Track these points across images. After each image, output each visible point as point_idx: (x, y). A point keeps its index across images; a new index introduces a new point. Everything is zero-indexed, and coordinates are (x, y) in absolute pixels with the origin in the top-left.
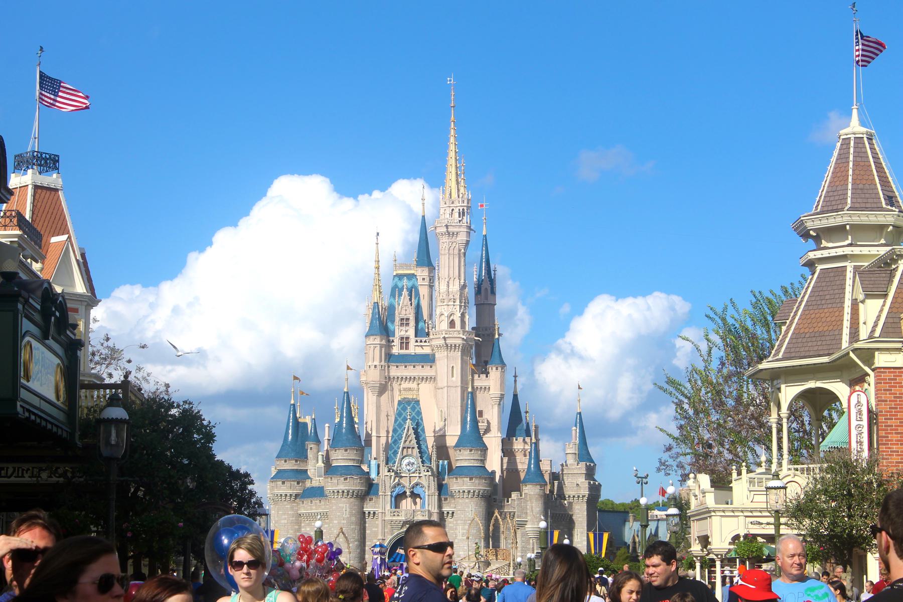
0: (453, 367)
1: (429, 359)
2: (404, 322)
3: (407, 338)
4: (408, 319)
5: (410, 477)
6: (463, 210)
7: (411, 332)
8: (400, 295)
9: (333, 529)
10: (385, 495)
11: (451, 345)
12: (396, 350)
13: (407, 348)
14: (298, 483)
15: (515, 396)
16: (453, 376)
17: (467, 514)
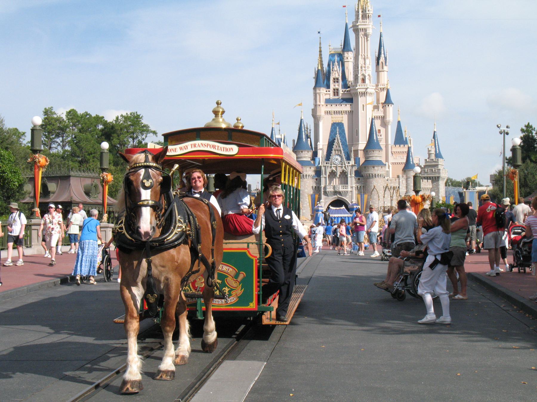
2: (336, 80)
3: (337, 90)
4: (338, 79)
5: (339, 167)
6: (368, 15)
8: (333, 65)
12: (332, 97)
13: (338, 95)
15: (399, 122)
16: (363, 110)
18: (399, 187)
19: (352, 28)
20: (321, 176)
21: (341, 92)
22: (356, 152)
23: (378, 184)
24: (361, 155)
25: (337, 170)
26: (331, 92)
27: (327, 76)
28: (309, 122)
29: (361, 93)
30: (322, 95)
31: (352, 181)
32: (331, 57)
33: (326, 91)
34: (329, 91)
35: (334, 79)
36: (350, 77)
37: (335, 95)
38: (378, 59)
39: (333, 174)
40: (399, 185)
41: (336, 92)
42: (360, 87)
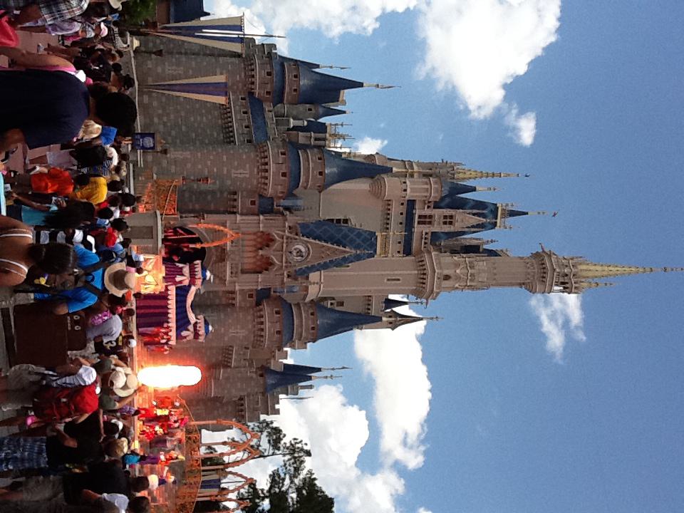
0: (399, 280)
1: (407, 251)
2: (449, 220)
4: (451, 223)
7: (436, 228)
9: (214, 153)
10: (259, 223)
11: (425, 279)
12: (417, 212)
14: (268, 93)
16: (388, 280)
17: (233, 328)
18: (230, 367)
19: (540, 251)
20: (261, 217)
21: (426, 229)
25: (274, 250)
26: (427, 212)
29: (425, 277)
30: (426, 197)
32: (492, 207)
33: (429, 202)
34: (428, 207)
35: (451, 217)
37: (420, 217)
39: (267, 241)
40: (235, 367)
41: (426, 220)
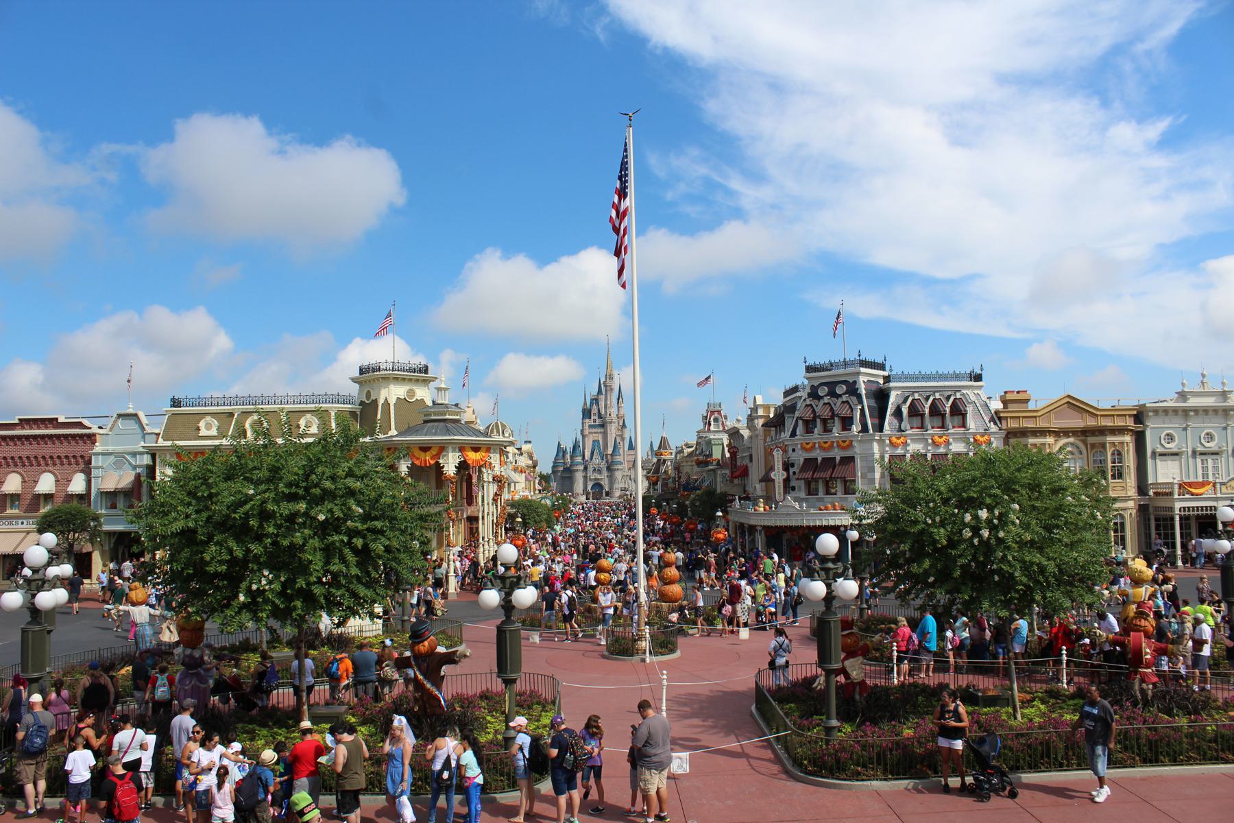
2: (595, 414)
22: (607, 455)
23: (618, 475)
24: (609, 457)
27: (590, 411)
28: (580, 438)
31: (605, 473)
36: (603, 412)
38: (618, 399)
41: (595, 421)
42: (608, 419)
